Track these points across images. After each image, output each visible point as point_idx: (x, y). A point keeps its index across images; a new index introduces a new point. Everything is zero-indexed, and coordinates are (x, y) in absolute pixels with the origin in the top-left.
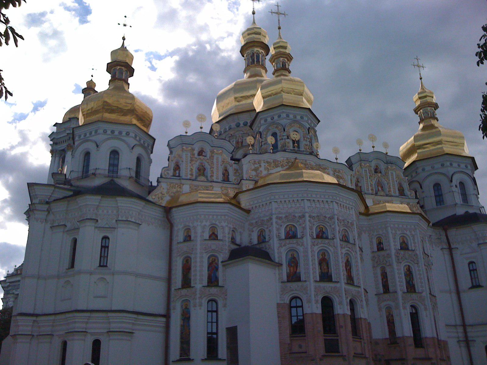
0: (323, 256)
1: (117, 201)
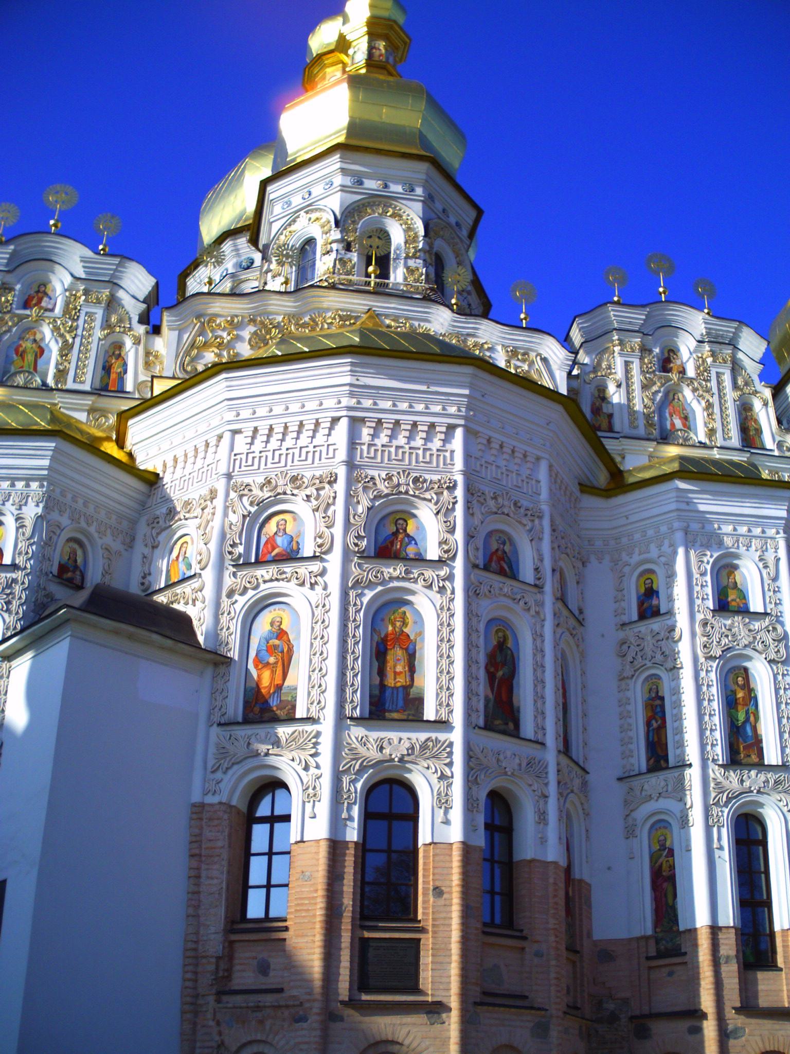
0: (398, 624)
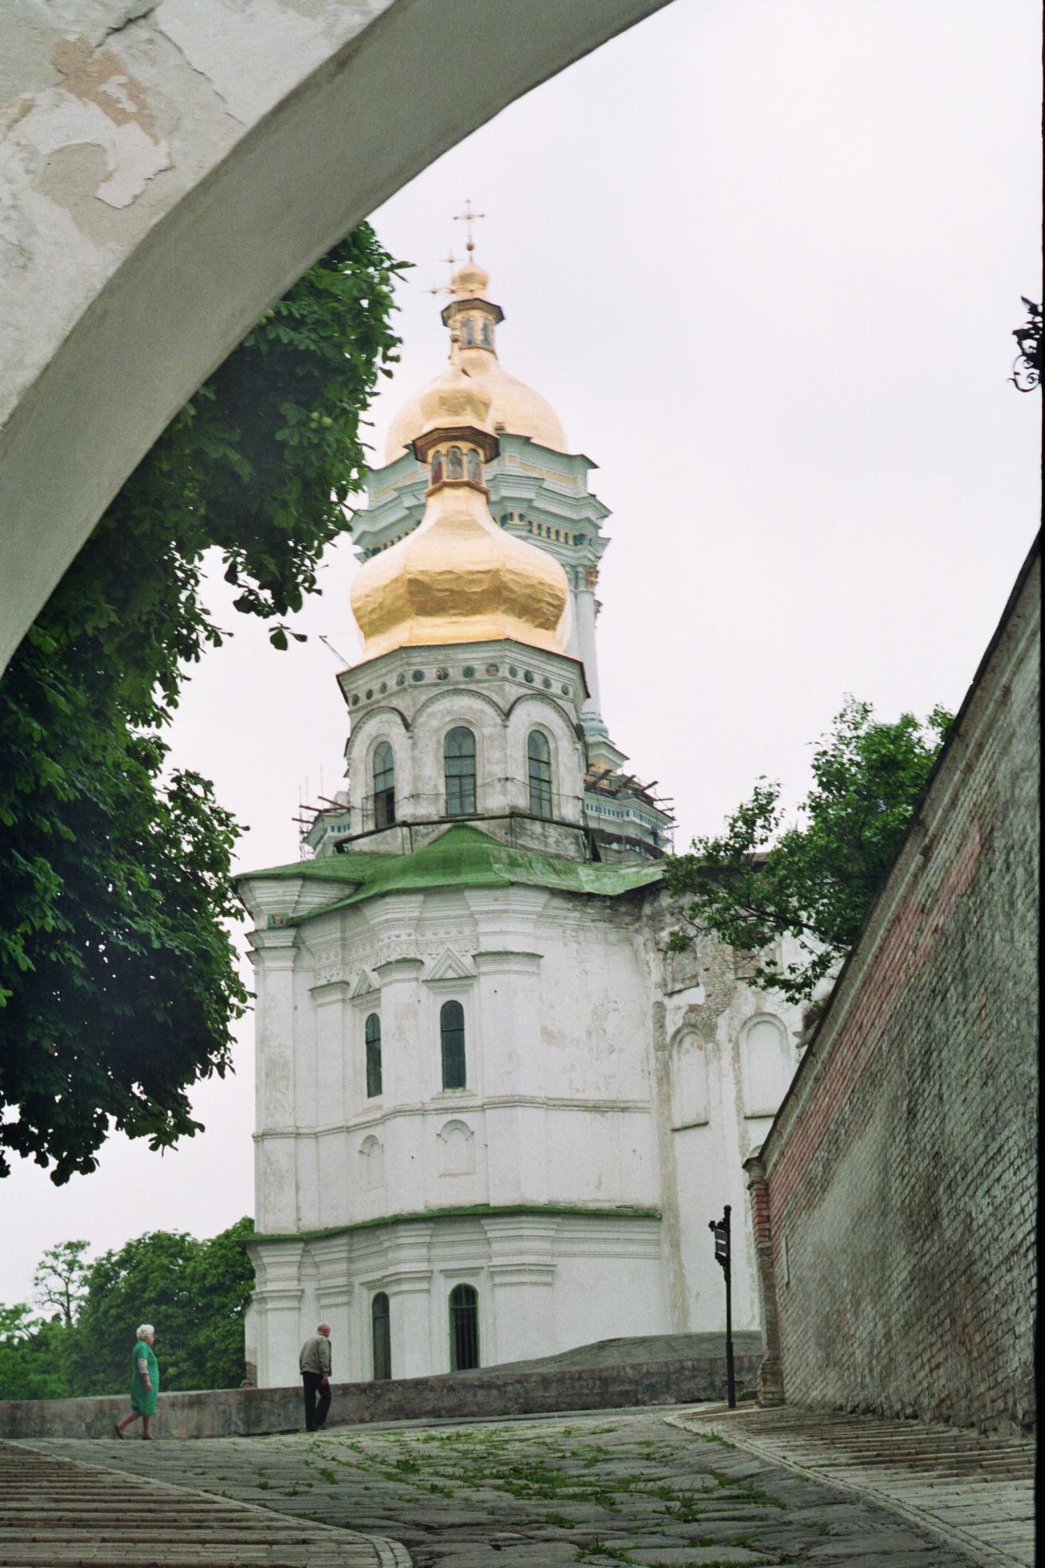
1: (465, 899)
